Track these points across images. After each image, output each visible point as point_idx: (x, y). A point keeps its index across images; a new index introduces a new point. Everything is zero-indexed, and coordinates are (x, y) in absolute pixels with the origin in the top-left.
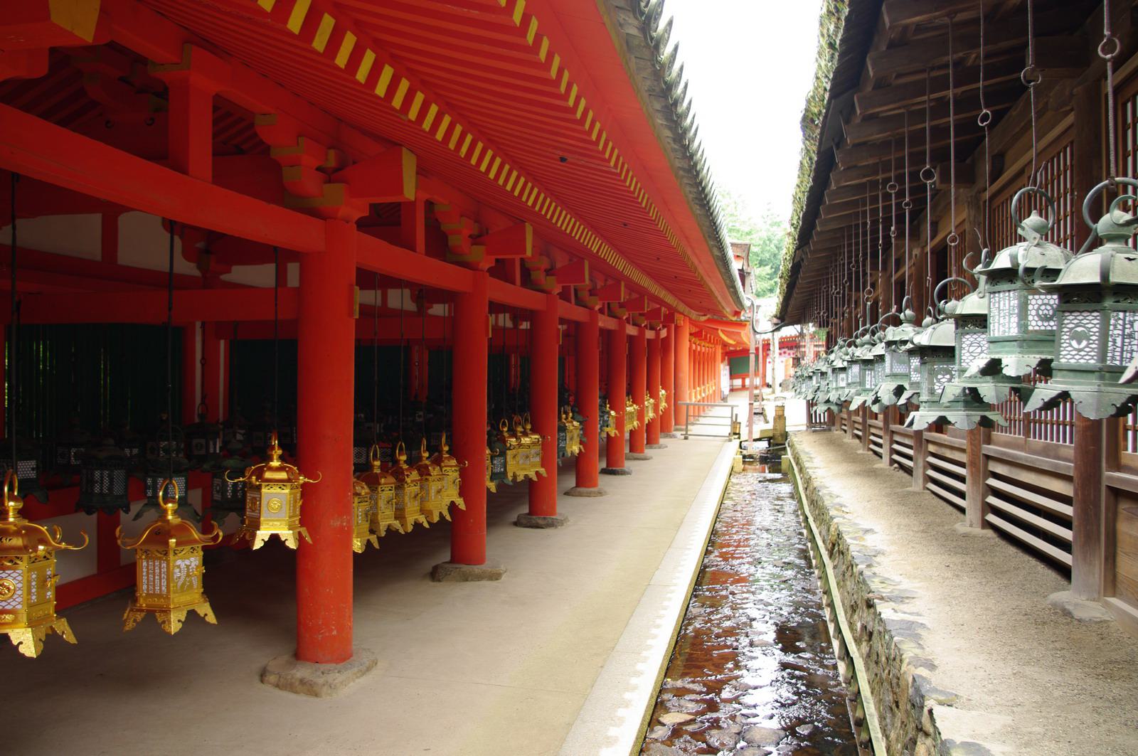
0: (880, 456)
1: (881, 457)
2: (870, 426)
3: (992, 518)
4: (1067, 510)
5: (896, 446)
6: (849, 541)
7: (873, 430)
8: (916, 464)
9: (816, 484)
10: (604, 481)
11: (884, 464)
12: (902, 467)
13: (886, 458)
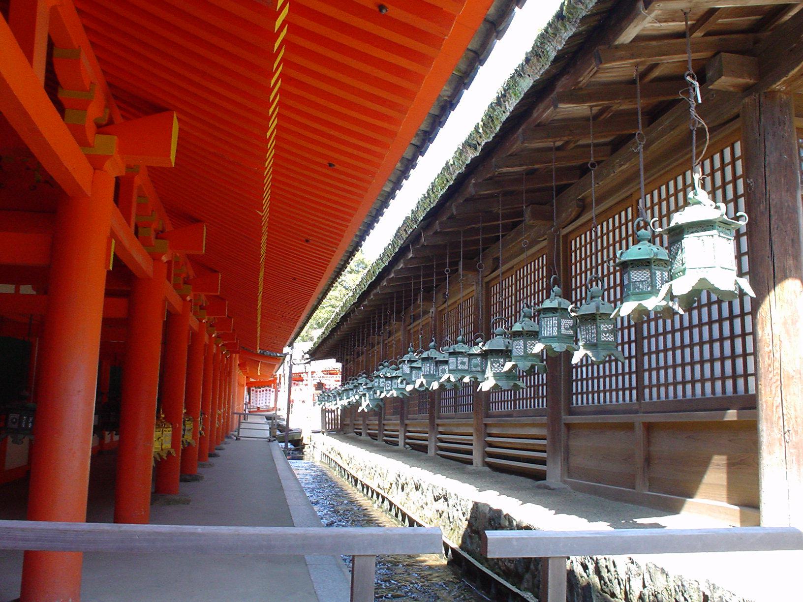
5: (408, 434)
13: (401, 443)
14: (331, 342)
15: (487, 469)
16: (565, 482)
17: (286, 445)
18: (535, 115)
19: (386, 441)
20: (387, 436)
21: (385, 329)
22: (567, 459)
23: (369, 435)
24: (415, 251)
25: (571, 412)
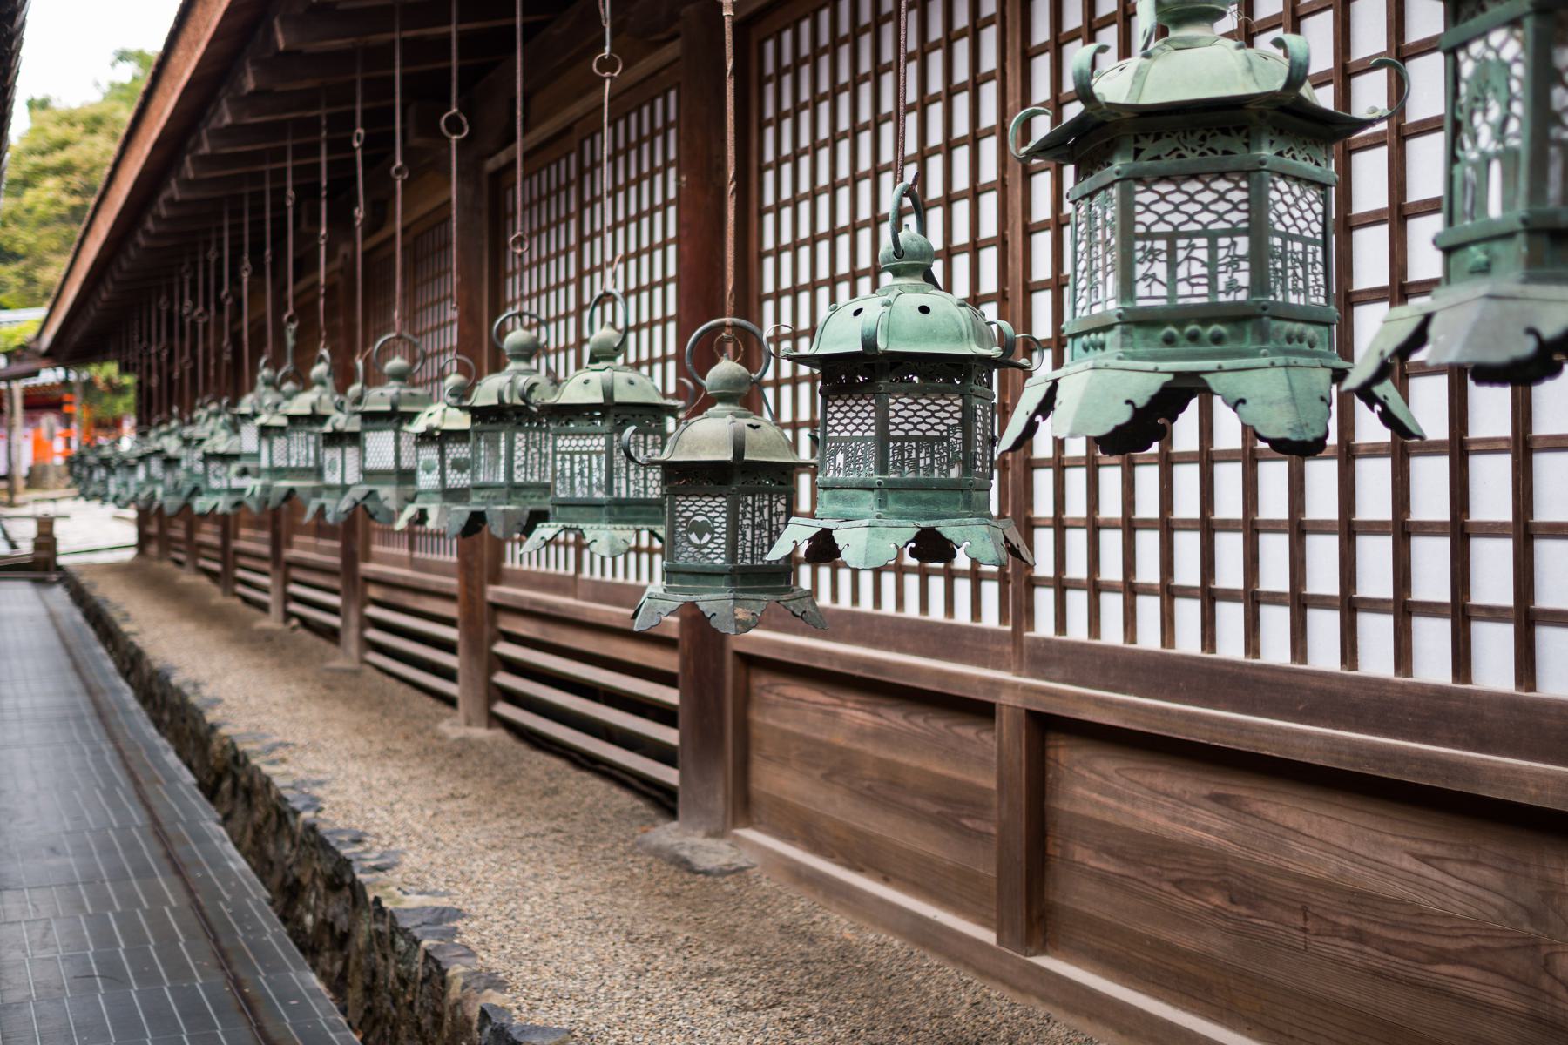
0: (263, 607)
3: (504, 709)
4: (671, 696)
5: (295, 589)
6: (266, 769)
7: (243, 561)
8: (345, 621)
9: (157, 665)
11: (271, 622)
13: (276, 611)
15: (500, 734)
19: (247, 600)
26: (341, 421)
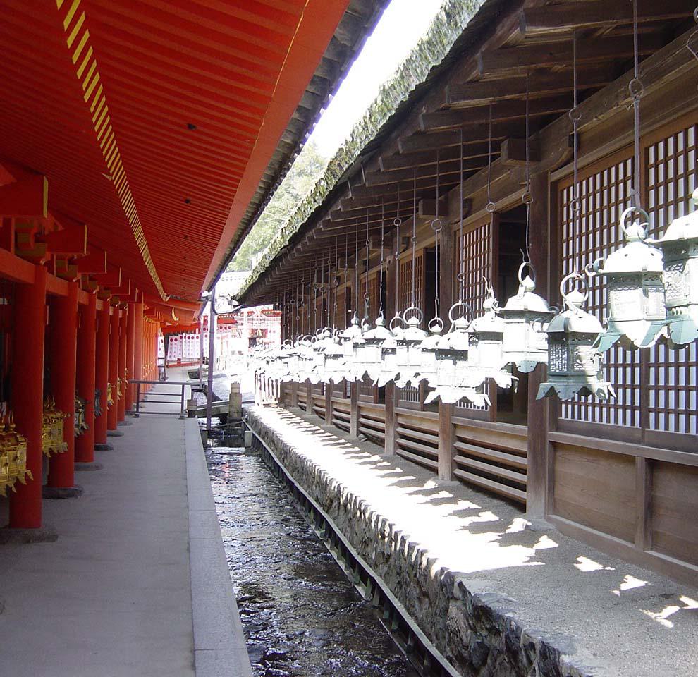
1: (349, 432)
2: (333, 402)
5: (362, 420)
10: (98, 456)
12: (369, 438)
13: (353, 431)
14: (268, 283)
15: (457, 483)
16: (549, 520)
17: (209, 422)
18: (499, 32)
19: (337, 425)
20: (337, 418)
21: (333, 275)
22: (552, 489)
23: (317, 412)
24: (354, 190)
25: (558, 426)
26: (390, 343)
